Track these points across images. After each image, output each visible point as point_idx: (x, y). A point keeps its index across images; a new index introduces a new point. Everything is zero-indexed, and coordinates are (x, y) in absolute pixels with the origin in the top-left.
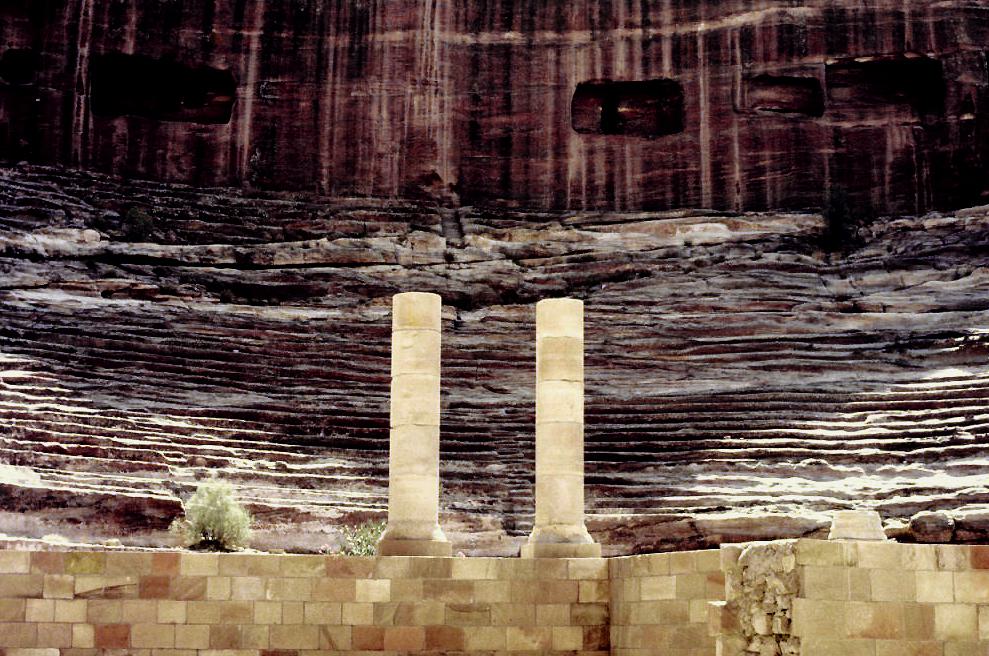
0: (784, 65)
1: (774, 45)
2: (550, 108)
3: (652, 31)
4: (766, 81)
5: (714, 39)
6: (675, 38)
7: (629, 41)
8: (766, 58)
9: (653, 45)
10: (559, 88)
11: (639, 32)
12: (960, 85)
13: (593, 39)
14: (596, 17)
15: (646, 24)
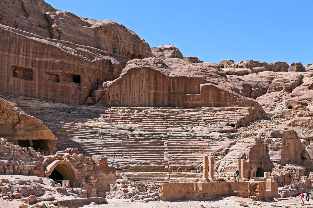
0: (52, 71)
1: (51, 66)
2: (6, 70)
3: (28, 57)
4: (49, 73)
5: (40, 62)
6: (32, 60)
7: (23, 58)
8: (49, 69)
9: (27, 61)
10: (8, 66)
11: (25, 57)
12: (84, 81)
13: (16, 56)
14: (17, 51)
15: (26, 55)
